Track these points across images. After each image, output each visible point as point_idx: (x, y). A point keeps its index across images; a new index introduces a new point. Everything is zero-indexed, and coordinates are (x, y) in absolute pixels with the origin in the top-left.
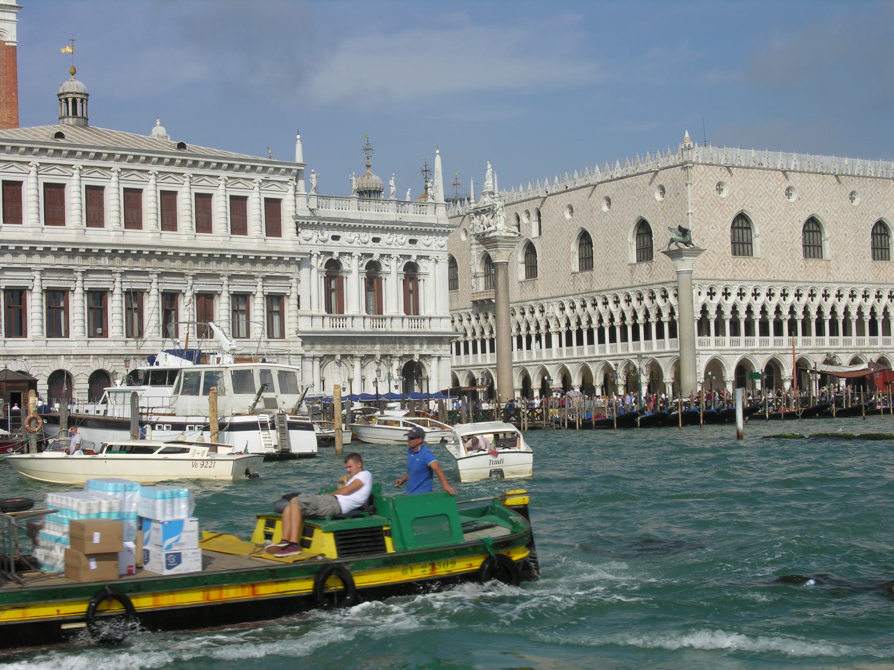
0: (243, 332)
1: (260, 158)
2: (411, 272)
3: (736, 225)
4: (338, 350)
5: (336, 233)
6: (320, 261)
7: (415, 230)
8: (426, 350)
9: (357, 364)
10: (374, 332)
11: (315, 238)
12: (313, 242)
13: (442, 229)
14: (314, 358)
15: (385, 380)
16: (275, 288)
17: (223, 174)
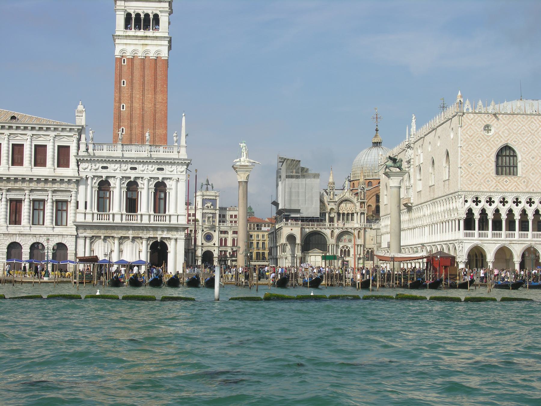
0: (64, 223)
1: (69, 124)
2: (160, 188)
3: (504, 154)
4: (102, 233)
5: (105, 165)
6: (94, 181)
7: (161, 164)
8: (165, 235)
9: (116, 242)
10: (127, 223)
11: (90, 168)
12: (88, 170)
13: (180, 161)
14: (85, 237)
15: (136, 252)
16: (60, 197)
17: (30, 133)
